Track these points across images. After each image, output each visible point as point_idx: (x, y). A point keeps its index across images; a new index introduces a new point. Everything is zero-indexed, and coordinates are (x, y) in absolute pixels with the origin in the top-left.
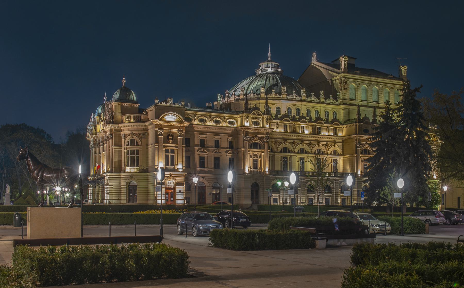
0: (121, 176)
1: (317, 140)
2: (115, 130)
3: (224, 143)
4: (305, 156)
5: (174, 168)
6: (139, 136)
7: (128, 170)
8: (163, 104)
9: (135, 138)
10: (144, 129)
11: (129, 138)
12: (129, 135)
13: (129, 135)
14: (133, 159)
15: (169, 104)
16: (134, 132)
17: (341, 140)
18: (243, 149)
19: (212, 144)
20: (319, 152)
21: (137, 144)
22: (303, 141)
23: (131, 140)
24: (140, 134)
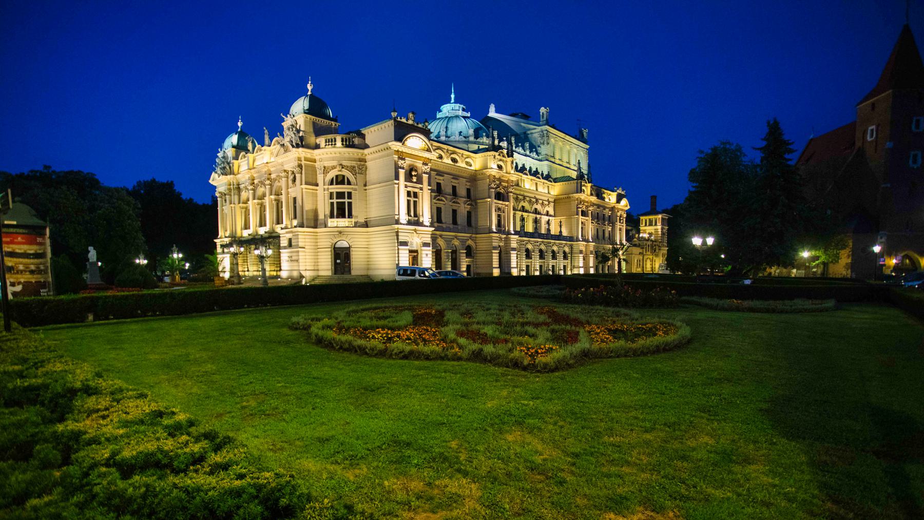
2: (306, 159)
3: (462, 191)
4: (525, 214)
5: (418, 220)
7: (333, 222)
8: (404, 120)
9: (346, 173)
11: (332, 174)
12: (334, 168)
13: (334, 168)
14: (341, 207)
15: (410, 122)
16: (345, 163)
19: (450, 191)
20: (536, 212)
21: (349, 183)
22: (525, 197)
23: (337, 176)
24: (354, 167)
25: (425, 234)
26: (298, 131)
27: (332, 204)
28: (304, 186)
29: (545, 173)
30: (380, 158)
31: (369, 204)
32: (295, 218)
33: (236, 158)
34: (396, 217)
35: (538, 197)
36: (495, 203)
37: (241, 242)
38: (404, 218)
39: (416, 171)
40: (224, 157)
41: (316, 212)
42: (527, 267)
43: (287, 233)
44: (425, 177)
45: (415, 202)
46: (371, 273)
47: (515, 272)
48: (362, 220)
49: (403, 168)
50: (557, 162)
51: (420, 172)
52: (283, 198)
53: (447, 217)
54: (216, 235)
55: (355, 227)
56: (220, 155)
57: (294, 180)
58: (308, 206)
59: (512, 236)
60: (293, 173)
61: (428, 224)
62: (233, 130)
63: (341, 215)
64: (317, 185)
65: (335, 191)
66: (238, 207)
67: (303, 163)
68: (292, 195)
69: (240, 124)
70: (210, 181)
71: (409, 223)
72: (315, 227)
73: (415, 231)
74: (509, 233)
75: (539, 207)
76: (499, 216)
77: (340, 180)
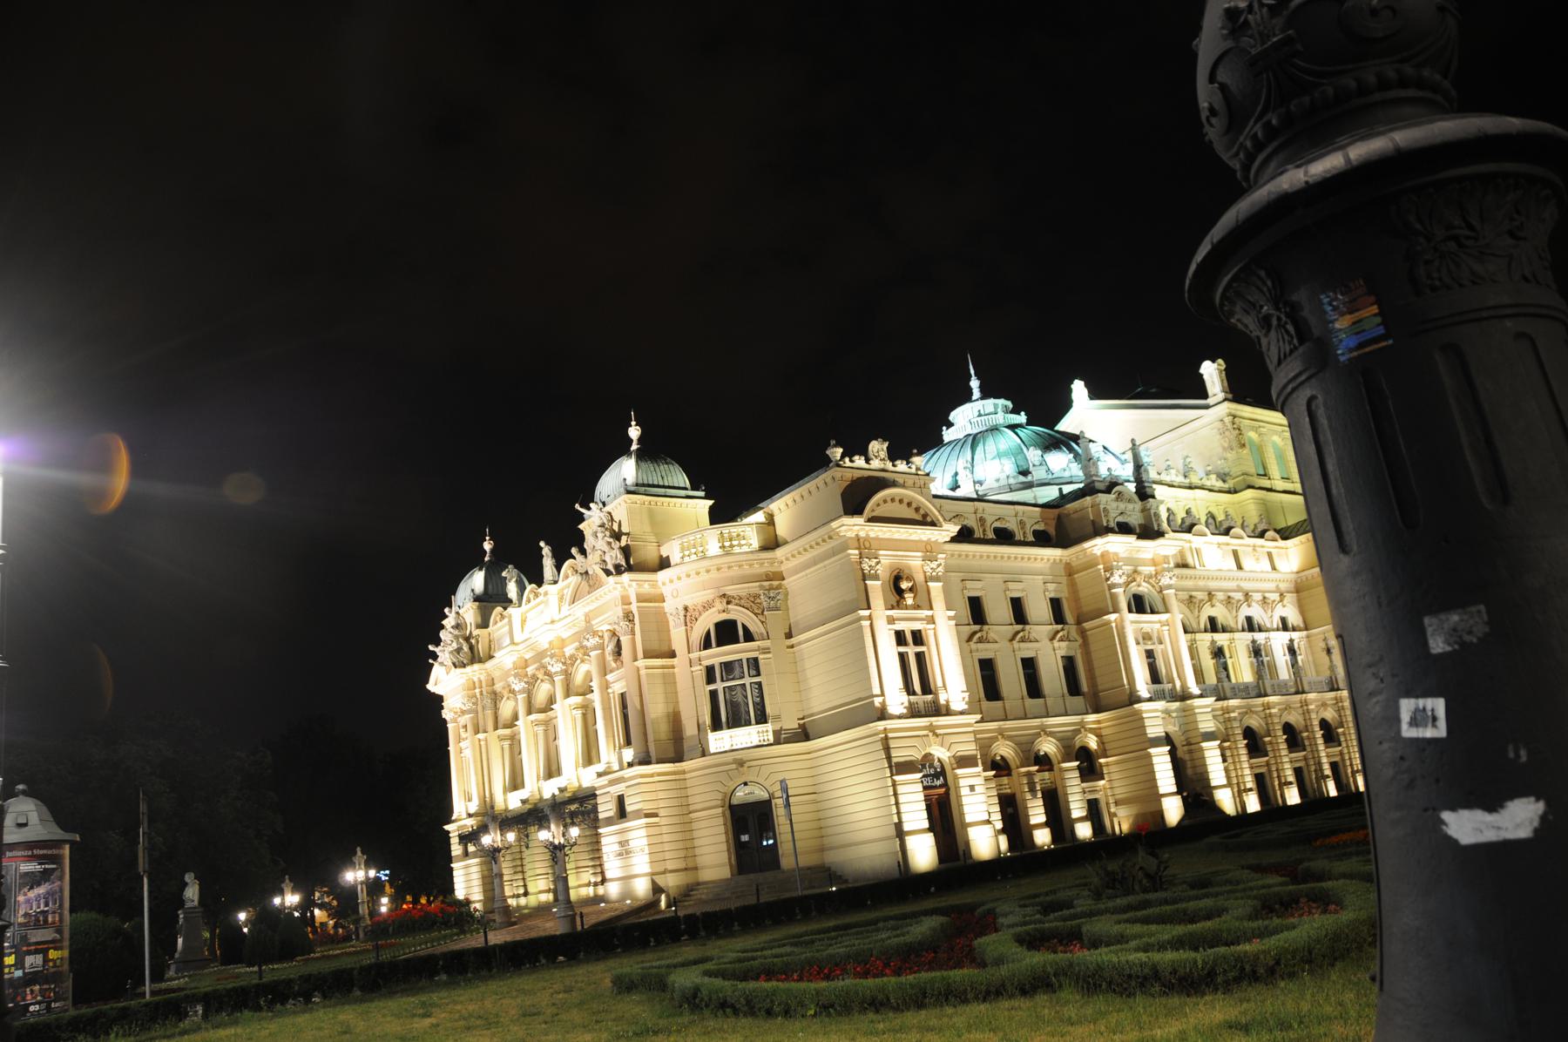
0: (684, 772)
1: (1239, 589)
2: (641, 599)
3: (1038, 609)
4: (1221, 639)
6: (751, 603)
7: (720, 741)
10: (769, 577)
11: (707, 621)
13: (707, 606)
15: (876, 464)
16: (731, 590)
17: (1291, 586)
18: (1113, 617)
20: (1251, 625)
21: (749, 637)
23: (719, 625)
24: (757, 596)
25: (957, 734)
26: (617, 536)
27: (713, 694)
28: (641, 663)
29: (1253, 517)
30: (814, 562)
31: (805, 678)
32: (628, 743)
33: (484, 624)
34: (877, 701)
35: (1246, 586)
36: (1132, 624)
37: (507, 821)
38: (896, 700)
39: (909, 579)
40: (457, 626)
41: (675, 721)
42: (1260, 780)
43: (612, 783)
44: (935, 587)
45: (920, 657)
46: (832, 858)
47: (1226, 801)
48: (791, 724)
49: (876, 577)
50: (1280, 485)
51: (919, 578)
52: (596, 697)
53: (1011, 680)
54: (446, 813)
55: (777, 742)
56: (448, 622)
57: (618, 651)
58: (657, 710)
59: (1197, 702)
60: (614, 634)
61: (962, 706)
62: (475, 561)
63: (737, 720)
64: (673, 655)
65: (716, 661)
66: (493, 736)
67: (634, 608)
68: (618, 688)
69: (487, 546)
70: (430, 687)
71: (914, 712)
72: (679, 758)
73: (932, 729)
74: (1185, 696)
75: (1257, 613)
76: (1150, 654)
77: (726, 632)
